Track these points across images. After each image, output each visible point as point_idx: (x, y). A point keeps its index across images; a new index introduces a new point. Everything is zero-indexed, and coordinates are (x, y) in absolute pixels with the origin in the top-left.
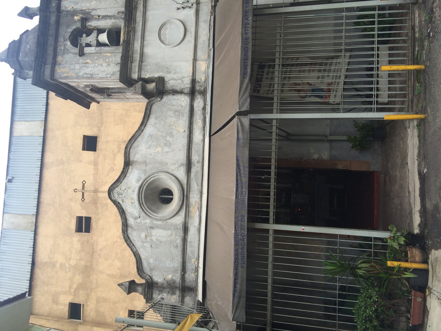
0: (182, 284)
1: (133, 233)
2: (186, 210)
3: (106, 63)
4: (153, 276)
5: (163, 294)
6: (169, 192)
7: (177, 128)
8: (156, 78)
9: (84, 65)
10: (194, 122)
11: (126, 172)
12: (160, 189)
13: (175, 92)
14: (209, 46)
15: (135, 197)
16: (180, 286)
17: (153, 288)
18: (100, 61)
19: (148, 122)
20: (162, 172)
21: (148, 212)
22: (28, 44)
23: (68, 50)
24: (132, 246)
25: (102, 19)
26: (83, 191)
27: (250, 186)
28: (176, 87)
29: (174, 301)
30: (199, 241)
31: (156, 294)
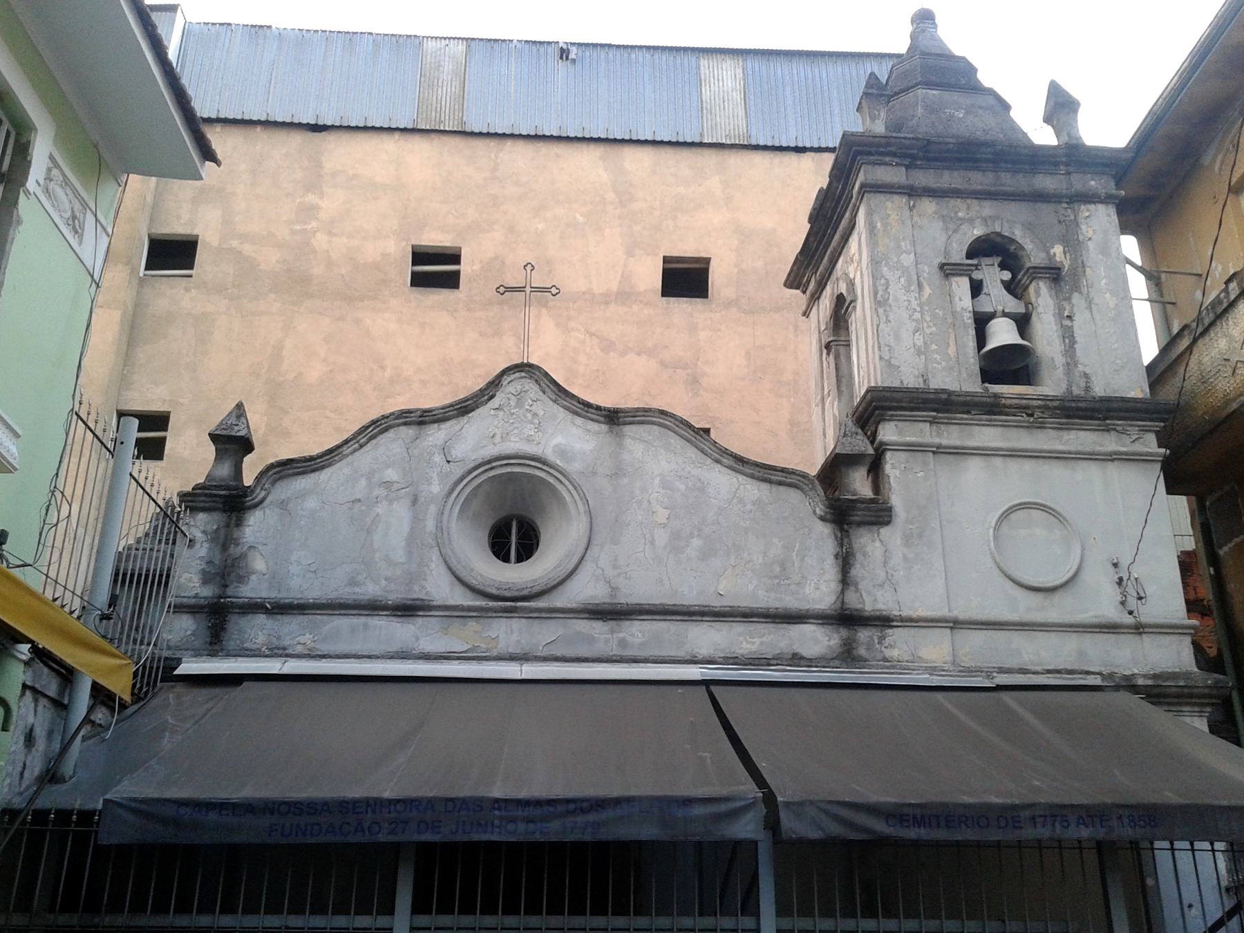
0: (233, 605)
1: (400, 441)
2: (470, 609)
3: (925, 343)
4: (262, 513)
5: (206, 545)
6: (528, 546)
7: (730, 570)
10: (752, 627)
11: (589, 415)
12: (538, 522)
13: (845, 561)
14: (1002, 671)
15: (512, 444)
16: (230, 597)
17: (224, 511)
19: (745, 478)
20: (589, 527)
21: (465, 485)
22: (967, 113)
23: (955, 231)
24: (358, 442)
26: (528, 289)
27: (535, 849)
28: (863, 567)
29: (182, 580)
30: (369, 657)
31: (208, 523)
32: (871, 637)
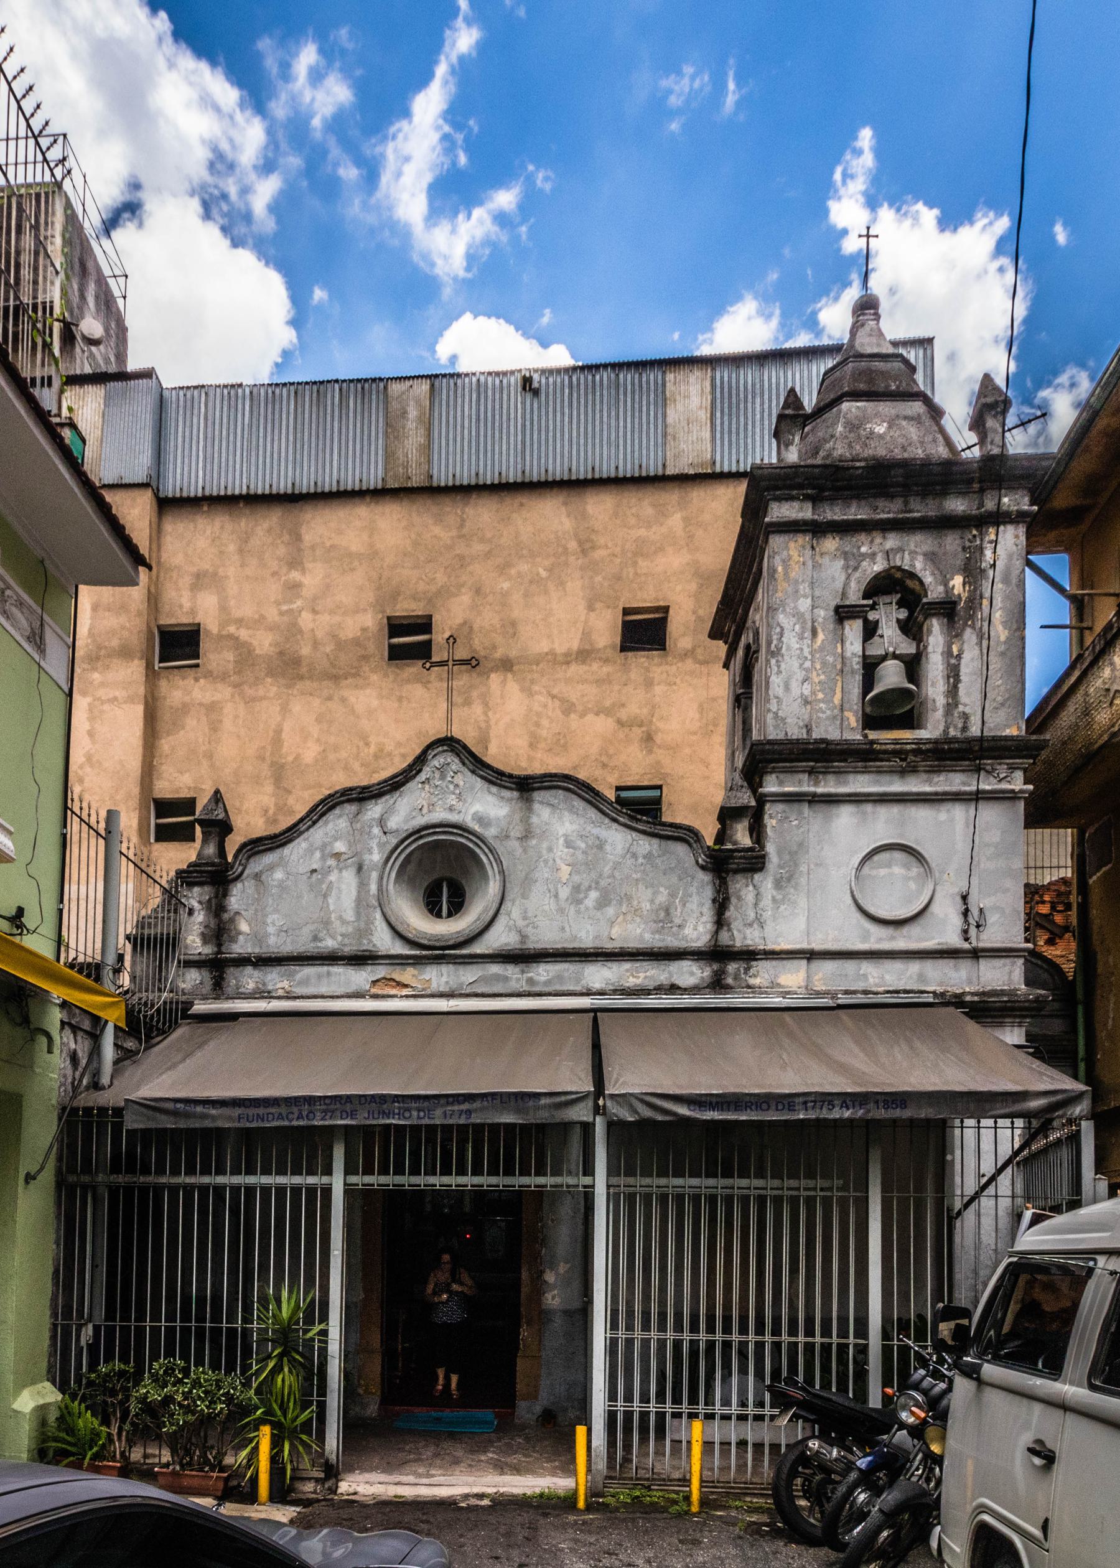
1: (345, 817)
5: (202, 913)
7: (621, 917)
8: (762, 847)
9: (810, 624)
10: (638, 964)
13: (721, 905)
14: (846, 992)
18: (818, 675)
21: (400, 854)
25: (949, 664)
29: (188, 941)
32: (738, 969)
